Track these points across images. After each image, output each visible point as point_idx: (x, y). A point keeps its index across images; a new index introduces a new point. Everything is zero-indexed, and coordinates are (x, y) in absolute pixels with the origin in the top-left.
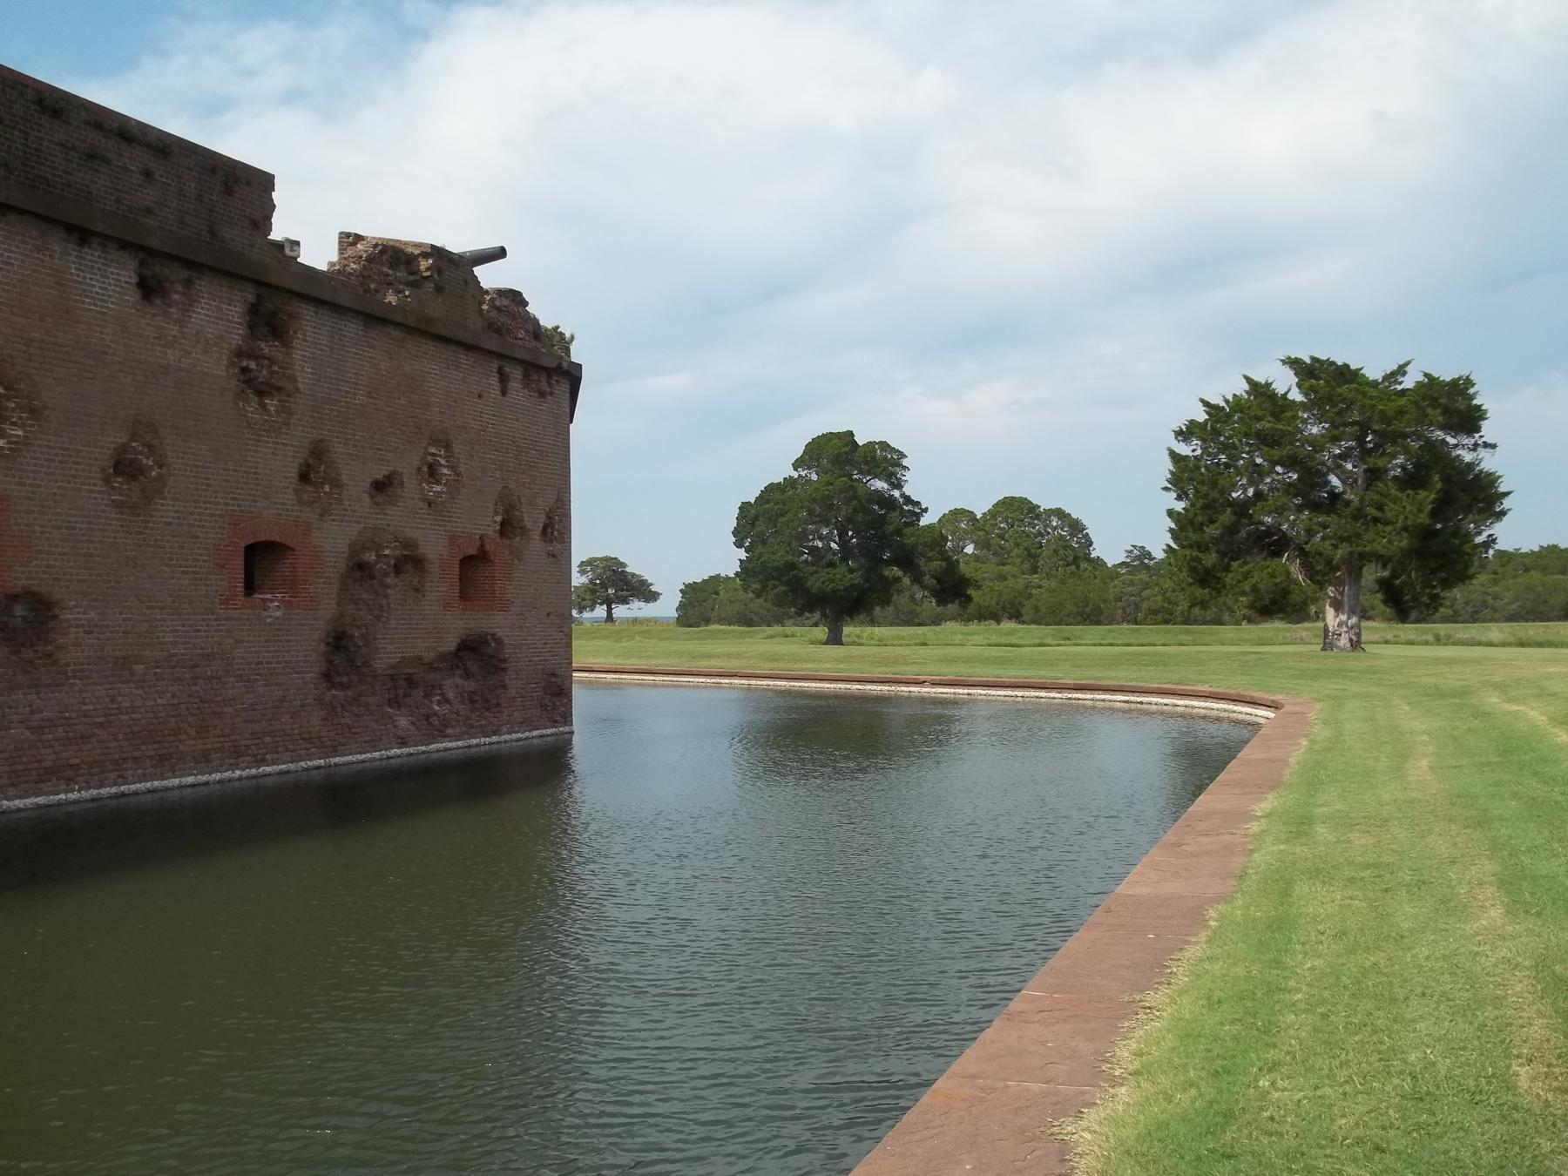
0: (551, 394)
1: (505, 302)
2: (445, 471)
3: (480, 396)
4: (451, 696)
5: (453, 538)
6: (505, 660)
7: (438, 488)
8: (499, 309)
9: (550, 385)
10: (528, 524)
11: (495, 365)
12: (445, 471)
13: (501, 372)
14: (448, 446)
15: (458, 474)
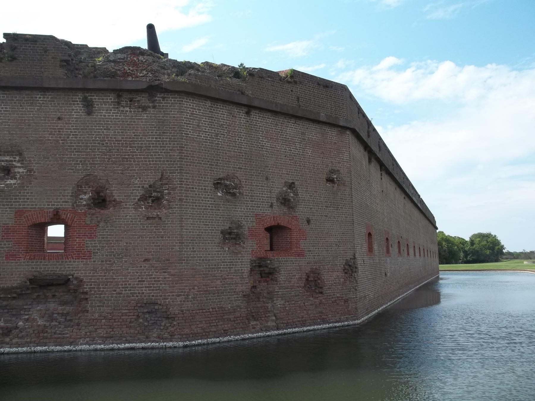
0: (154, 107)
1: (119, 56)
2: (21, 170)
3: (59, 119)
4: (35, 316)
5: (19, 213)
6: (86, 293)
7: (13, 182)
8: (114, 61)
9: (153, 102)
10: (118, 198)
11: (80, 96)
12: (17, 170)
13: (85, 99)
14: (20, 154)
15: (30, 171)
